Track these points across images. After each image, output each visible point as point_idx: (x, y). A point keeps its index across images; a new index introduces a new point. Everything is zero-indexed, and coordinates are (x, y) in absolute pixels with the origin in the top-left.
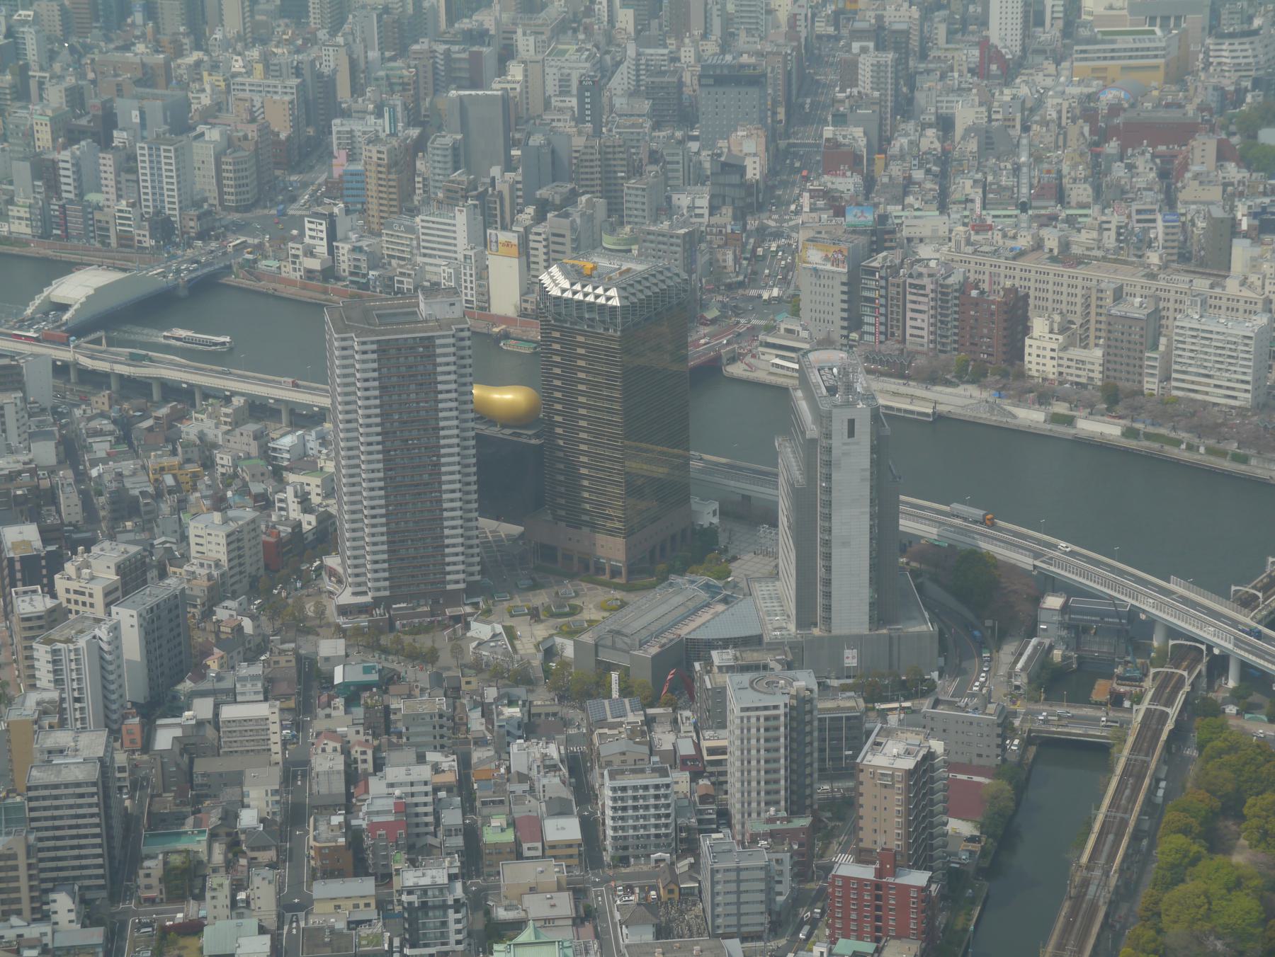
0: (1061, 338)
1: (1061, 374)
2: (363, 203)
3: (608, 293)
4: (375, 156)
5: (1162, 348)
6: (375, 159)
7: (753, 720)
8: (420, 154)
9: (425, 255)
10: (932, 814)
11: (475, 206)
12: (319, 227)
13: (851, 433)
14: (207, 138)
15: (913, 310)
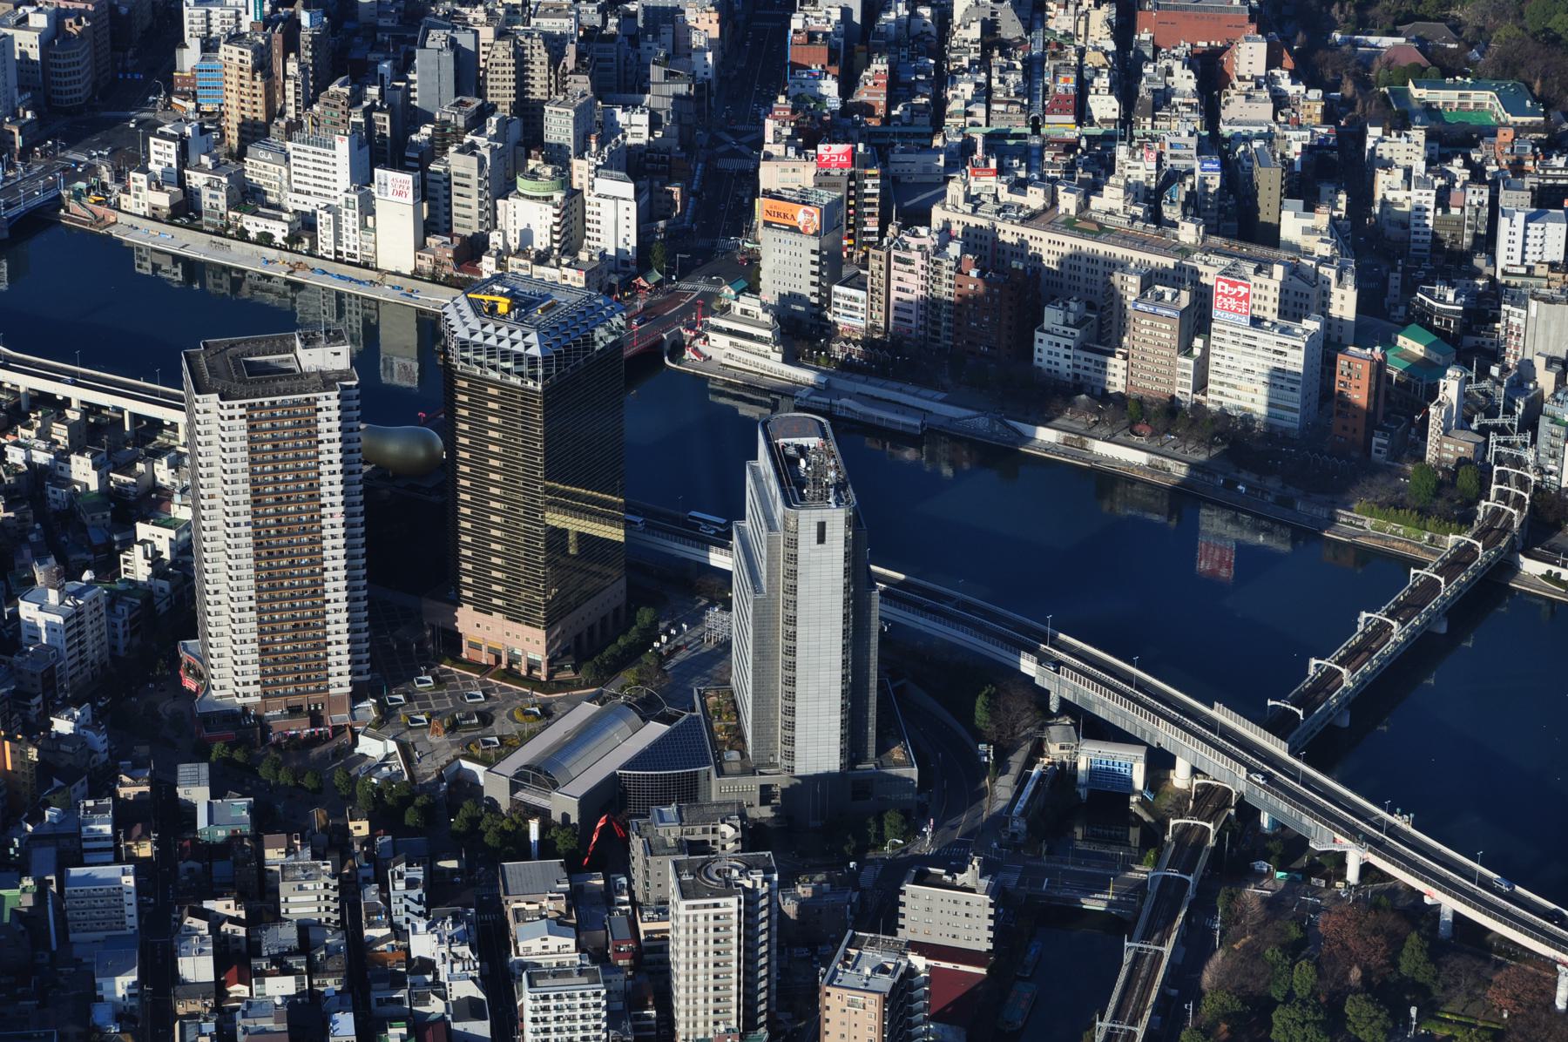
0: (1077, 332)
1: (1077, 376)
2: (221, 105)
3: (527, 339)
4: (236, 57)
5: (1197, 352)
6: (236, 61)
7: (701, 919)
8: (292, 55)
9: (297, 191)
10: (911, 1025)
11: (360, 124)
12: (168, 151)
13: (821, 539)
14: (31, 24)
15: (899, 289)
